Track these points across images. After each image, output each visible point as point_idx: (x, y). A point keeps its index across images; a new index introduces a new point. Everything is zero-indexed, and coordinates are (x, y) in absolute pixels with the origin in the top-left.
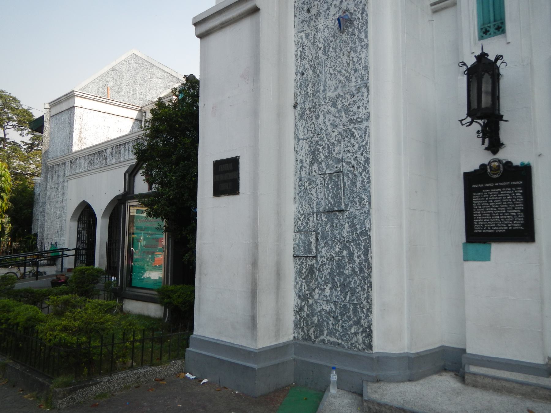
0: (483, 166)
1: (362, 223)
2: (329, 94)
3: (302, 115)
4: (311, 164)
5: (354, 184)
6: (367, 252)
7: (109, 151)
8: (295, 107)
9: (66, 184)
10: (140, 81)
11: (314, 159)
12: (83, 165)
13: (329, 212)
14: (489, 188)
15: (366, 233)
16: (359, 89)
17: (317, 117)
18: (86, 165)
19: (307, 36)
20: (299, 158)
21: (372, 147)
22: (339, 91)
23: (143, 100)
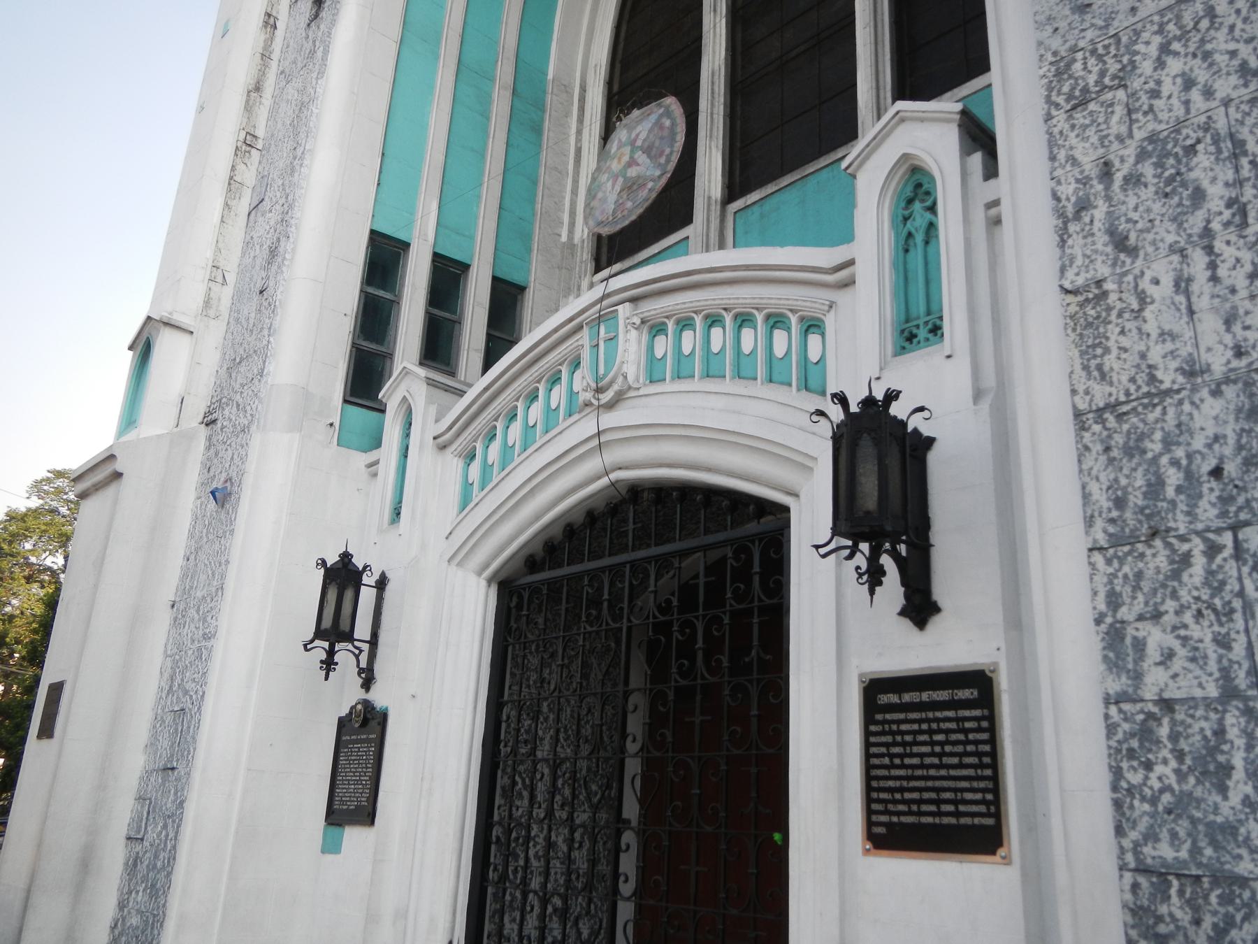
8: (173, 606)
13: (165, 769)
14: (357, 741)
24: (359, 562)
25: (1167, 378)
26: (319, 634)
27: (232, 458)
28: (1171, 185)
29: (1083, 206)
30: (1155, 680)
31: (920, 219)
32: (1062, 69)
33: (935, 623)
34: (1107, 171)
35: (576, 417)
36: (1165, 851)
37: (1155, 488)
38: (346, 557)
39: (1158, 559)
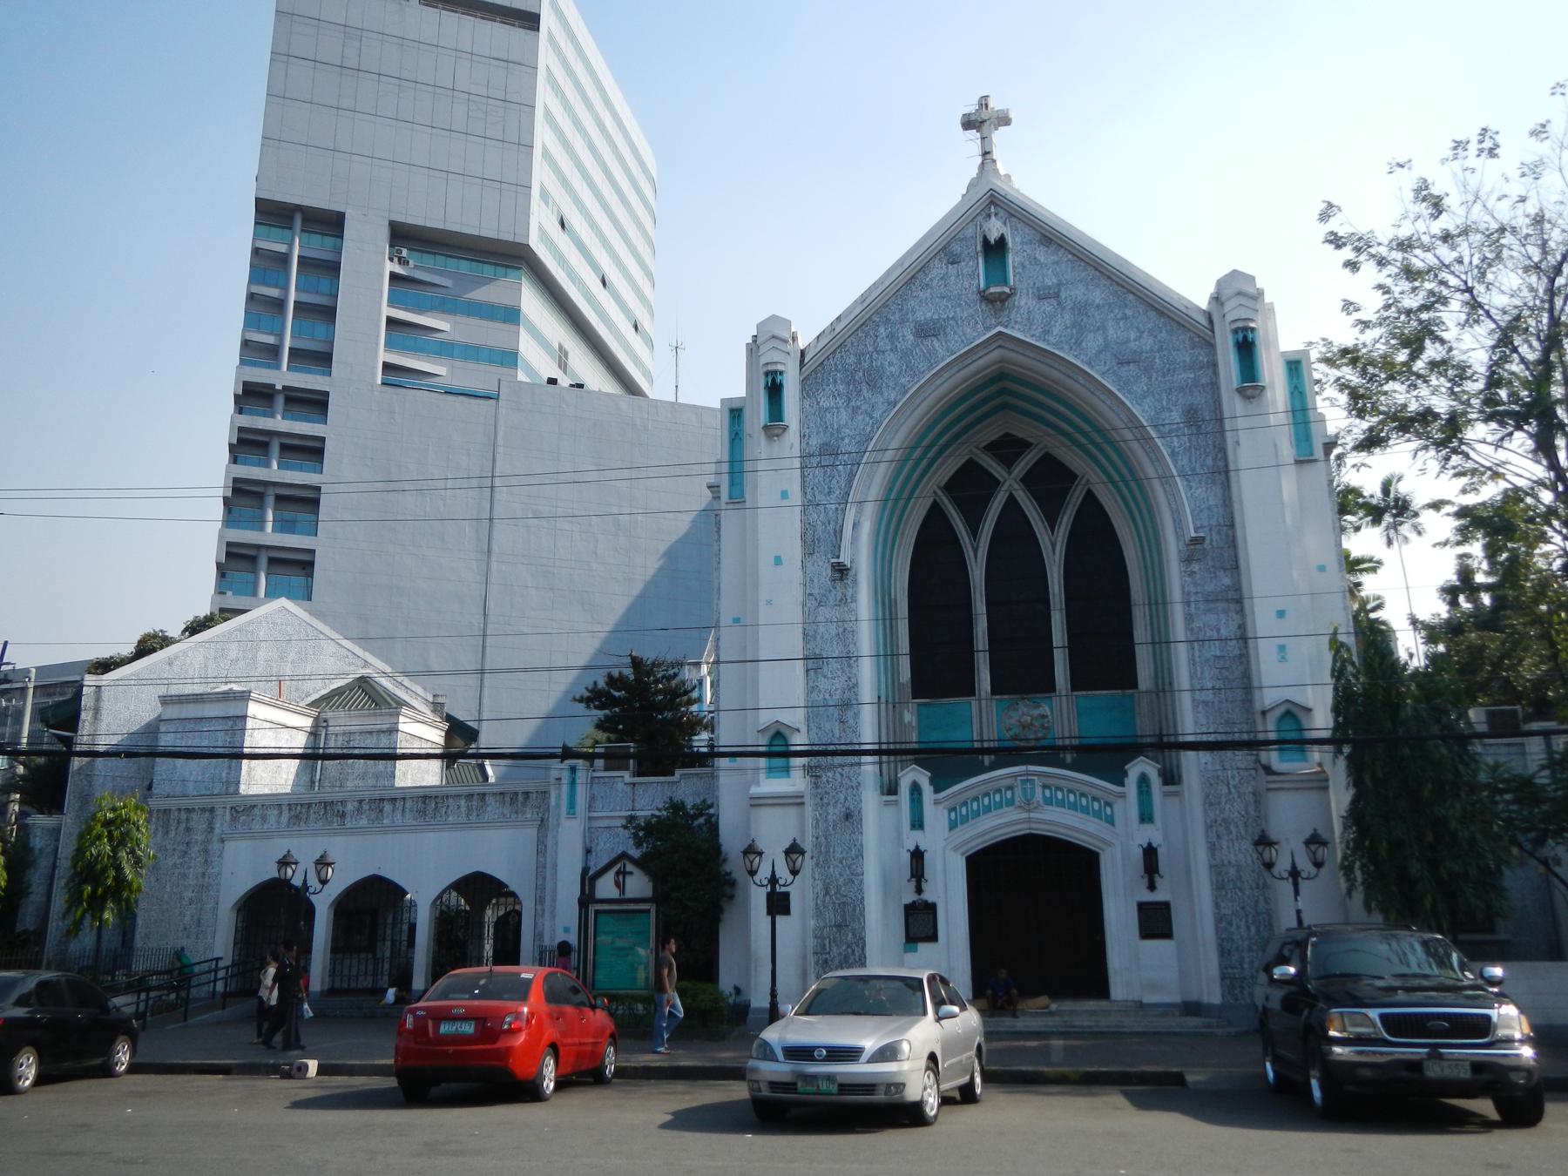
0: (914, 902)
1: (860, 933)
2: (837, 855)
3: (817, 864)
4: (825, 896)
5: (854, 910)
6: (863, 949)
7: (350, 807)
9: (216, 846)
10: (292, 656)
11: (827, 893)
12: (273, 819)
13: (839, 926)
15: (863, 939)
16: (857, 857)
17: (829, 868)
18: (284, 819)
19: (820, 815)
20: (816, 891)
21: (865, 889)
22: (844, 854)
23: (297, 690)
24: (922, 848)
25: (1226, 862)
26: (913, 876)
27: (846, 799)
28: (1227, 828)
29: (1211, 826)
30: (1223, 911)
31: (1144, 789)
32: (1208, 796)
33: (1156, 891)
34: (1216, 821)
35: (1011, 808)
36: (1223, 936)
37: (1223, 880)
38: (917, 847)
39: (1224, 893)
